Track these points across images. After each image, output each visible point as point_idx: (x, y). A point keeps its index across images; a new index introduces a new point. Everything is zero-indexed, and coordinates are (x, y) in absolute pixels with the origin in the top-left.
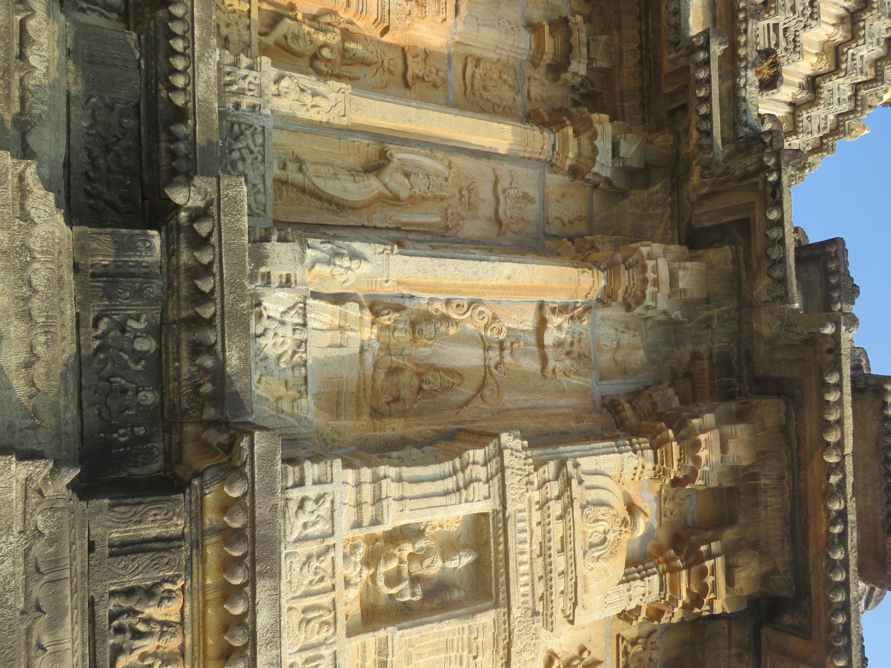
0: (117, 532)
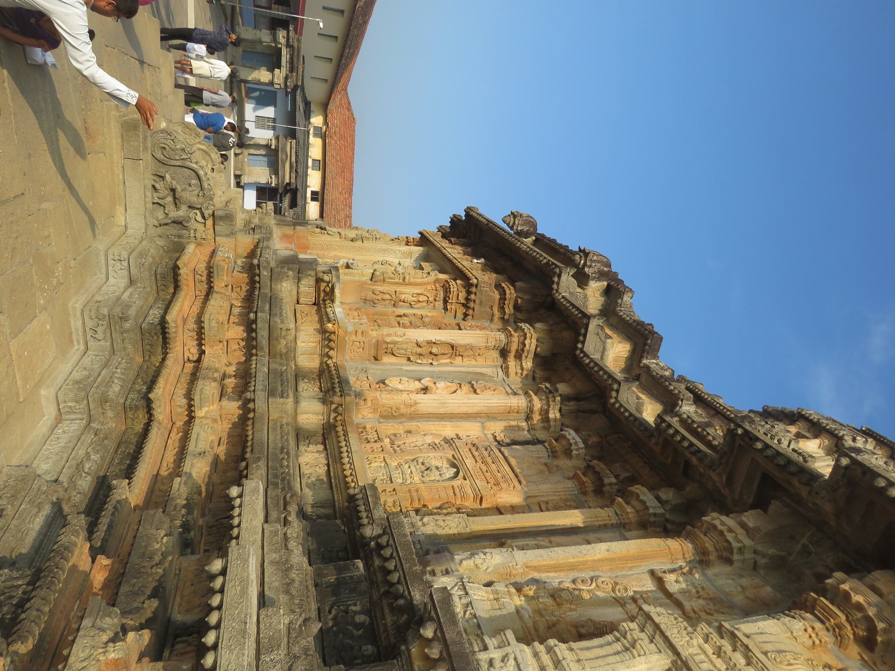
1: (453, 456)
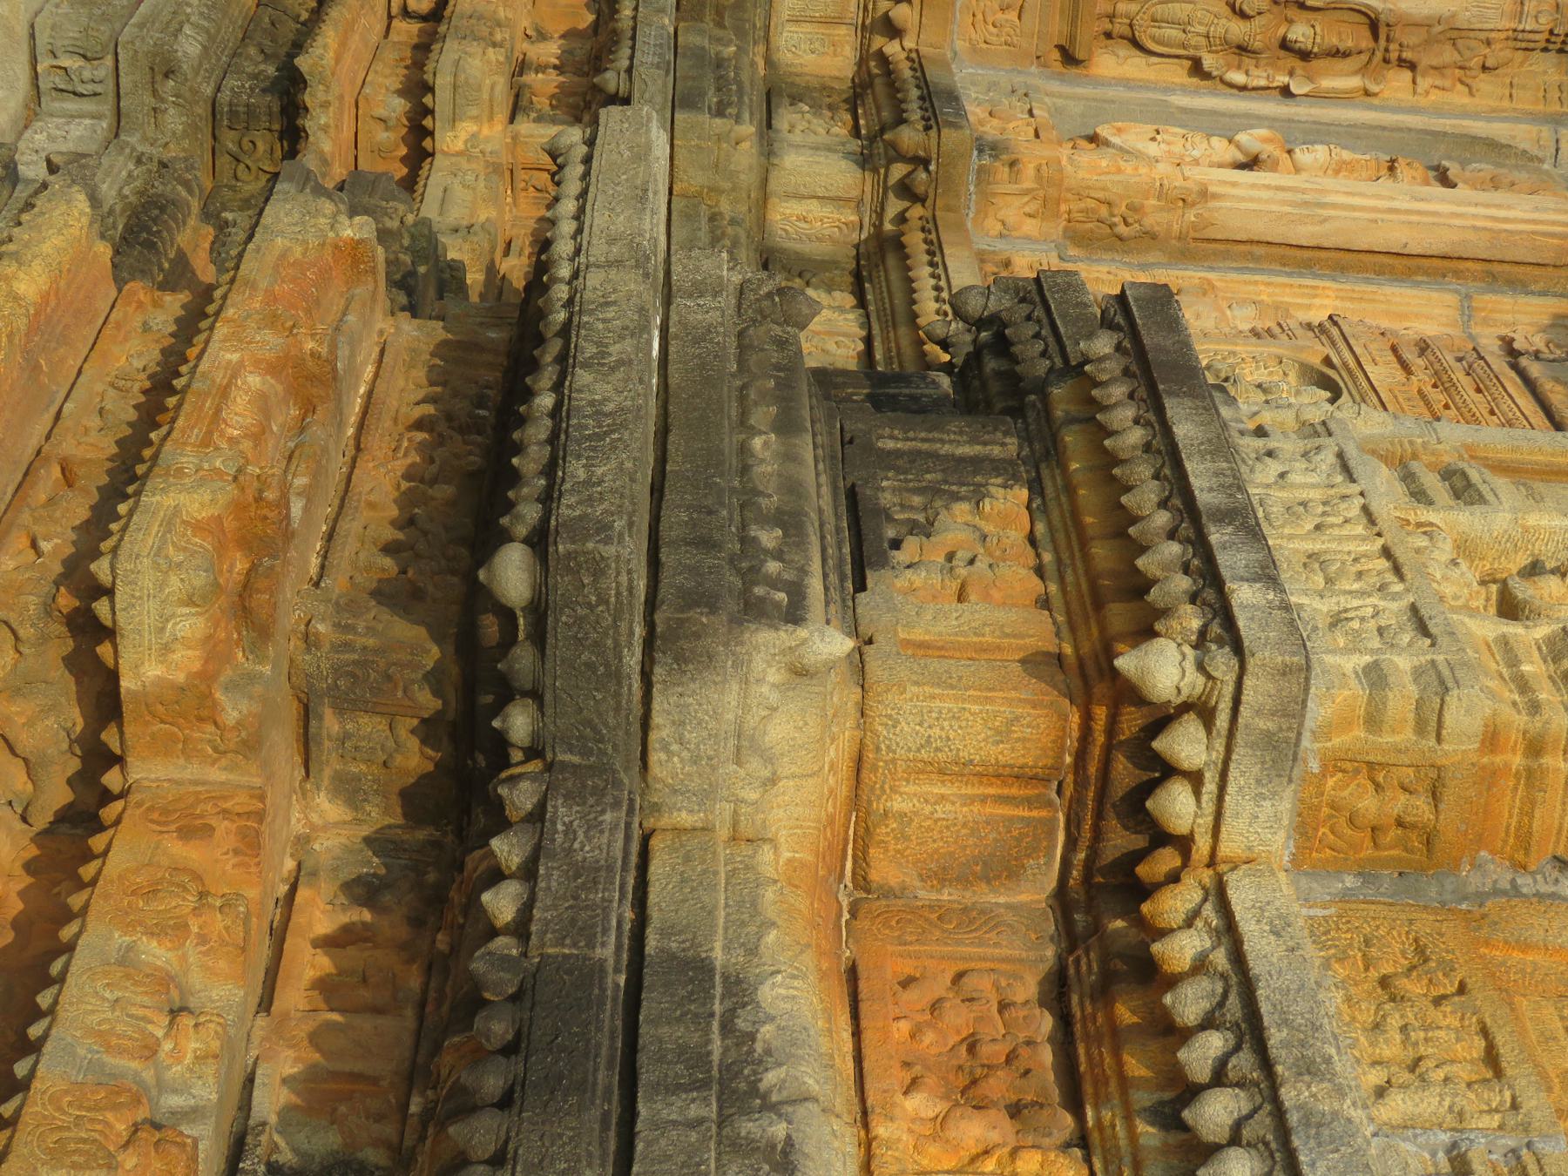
0: (892, 437)
1: (1327, 361)
